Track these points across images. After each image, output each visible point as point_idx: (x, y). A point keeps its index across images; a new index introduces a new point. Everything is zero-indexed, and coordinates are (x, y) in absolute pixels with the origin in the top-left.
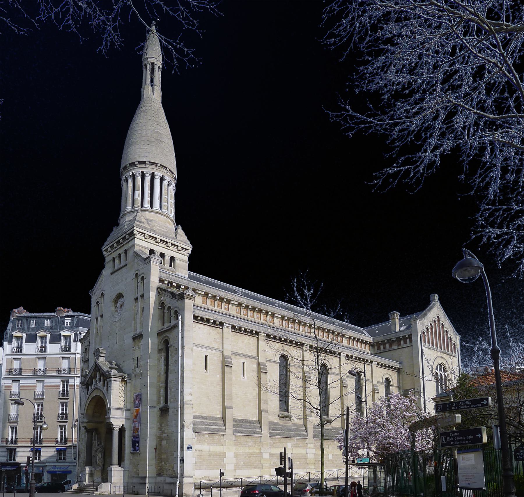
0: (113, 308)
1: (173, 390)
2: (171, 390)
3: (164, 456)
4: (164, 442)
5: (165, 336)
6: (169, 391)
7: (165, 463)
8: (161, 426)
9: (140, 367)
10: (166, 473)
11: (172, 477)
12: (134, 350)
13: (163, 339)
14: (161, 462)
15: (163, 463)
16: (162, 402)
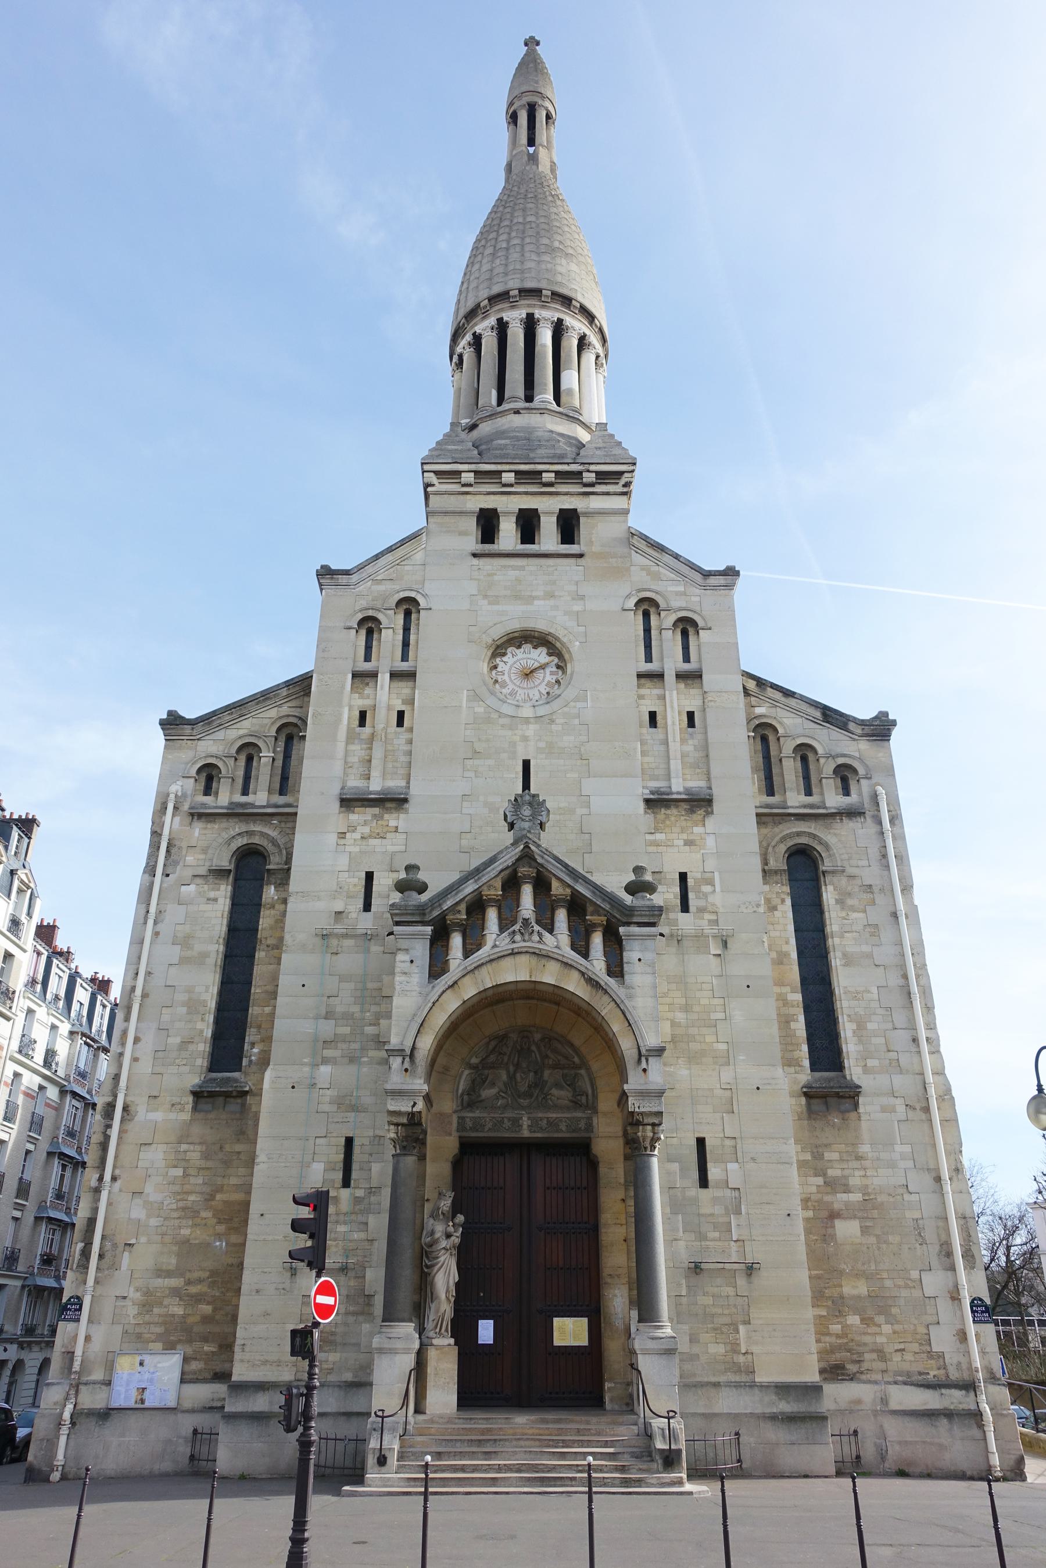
0: (485, 667)
1: (870, 1026)
2: (861, 1026)
3: (854, 1288)
4: (847, 1230)
5: (799, 834)
6: (847, 1029)
7: (867, 1321)
8: (818, 1156)
9: (701, 910)
10: (881, 1365)
11: (928, 1386)
12: (656, 844)
13: (783, 840)
14: (841, 1314)
15: (854, 1320)
16: (807, 1063)
